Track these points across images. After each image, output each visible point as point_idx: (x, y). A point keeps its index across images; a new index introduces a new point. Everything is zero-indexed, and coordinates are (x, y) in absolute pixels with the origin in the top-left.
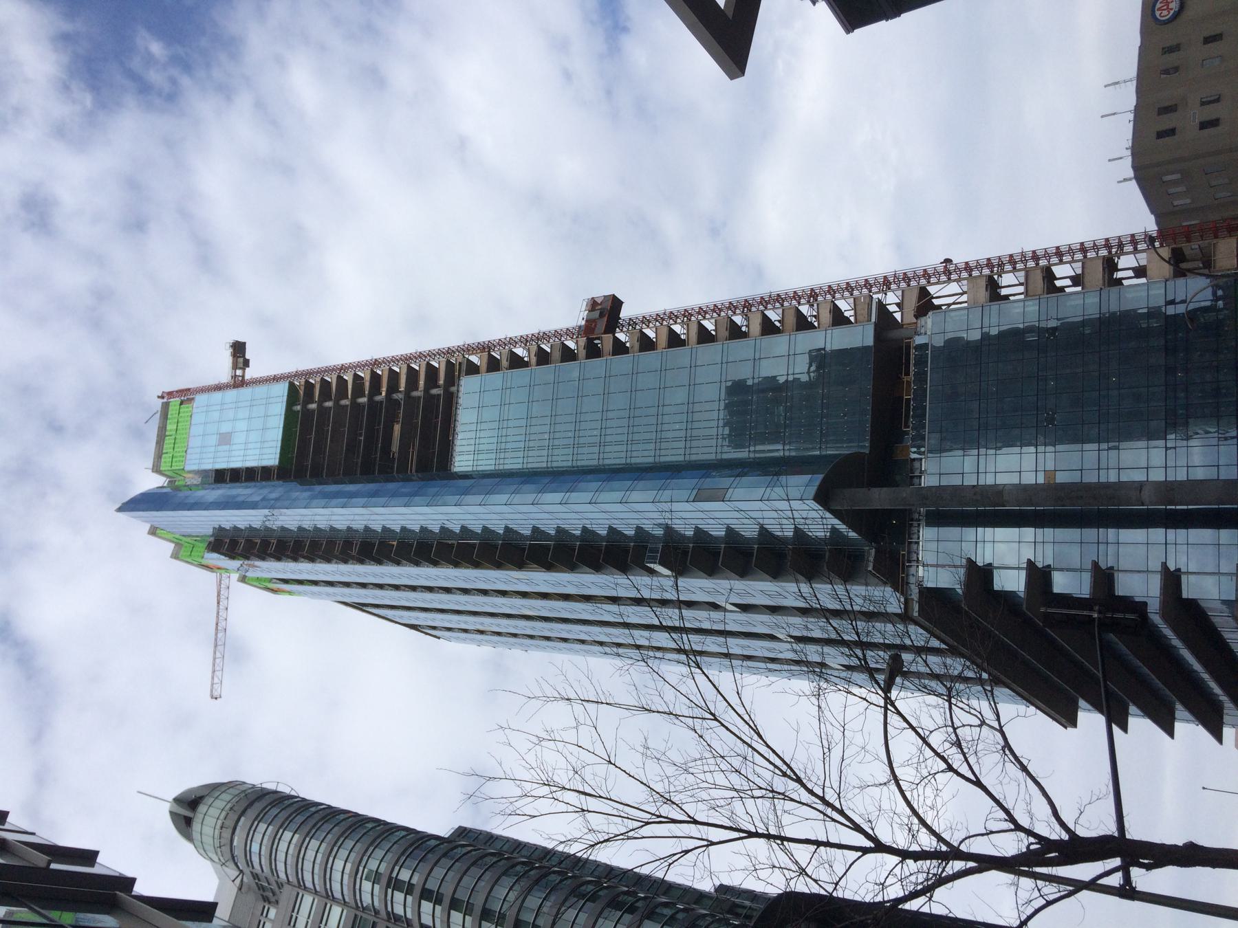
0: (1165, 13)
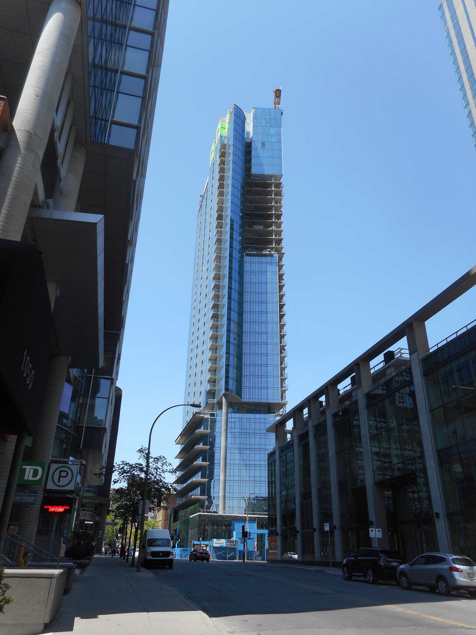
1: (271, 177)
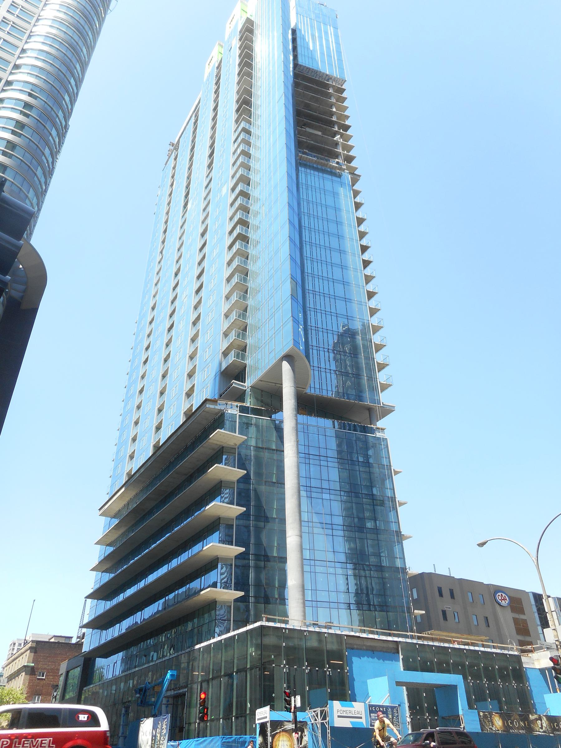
0: (500, 598)
1: (329, 78)
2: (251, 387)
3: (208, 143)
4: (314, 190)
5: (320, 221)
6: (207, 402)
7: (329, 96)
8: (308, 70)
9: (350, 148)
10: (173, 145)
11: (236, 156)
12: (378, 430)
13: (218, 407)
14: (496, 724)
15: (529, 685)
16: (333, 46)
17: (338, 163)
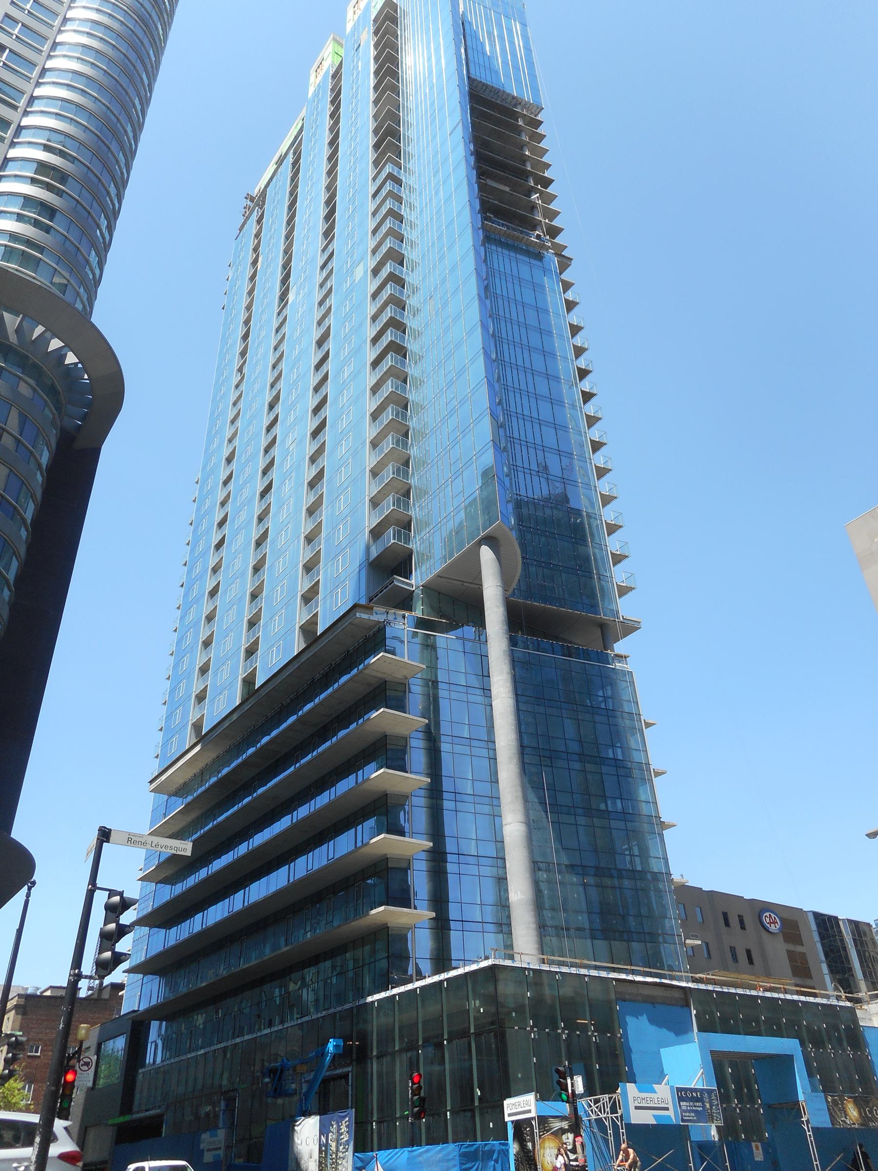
0: (768, 920)
1: (517, 101)
2: (422, 586)
3: (323, 197)
4: (503, 278)
5: (516, 328)
6: (357, 609)
7: (518, 130)
8: (485, 87)
9: (554, 214)
10: (252, 199)
11: (379, 217)
12: (617, 658)
13: (374, 618)
14: (850, 1114)
15: (869, 1054)
16: (521, 52)
17: (538, 237)
